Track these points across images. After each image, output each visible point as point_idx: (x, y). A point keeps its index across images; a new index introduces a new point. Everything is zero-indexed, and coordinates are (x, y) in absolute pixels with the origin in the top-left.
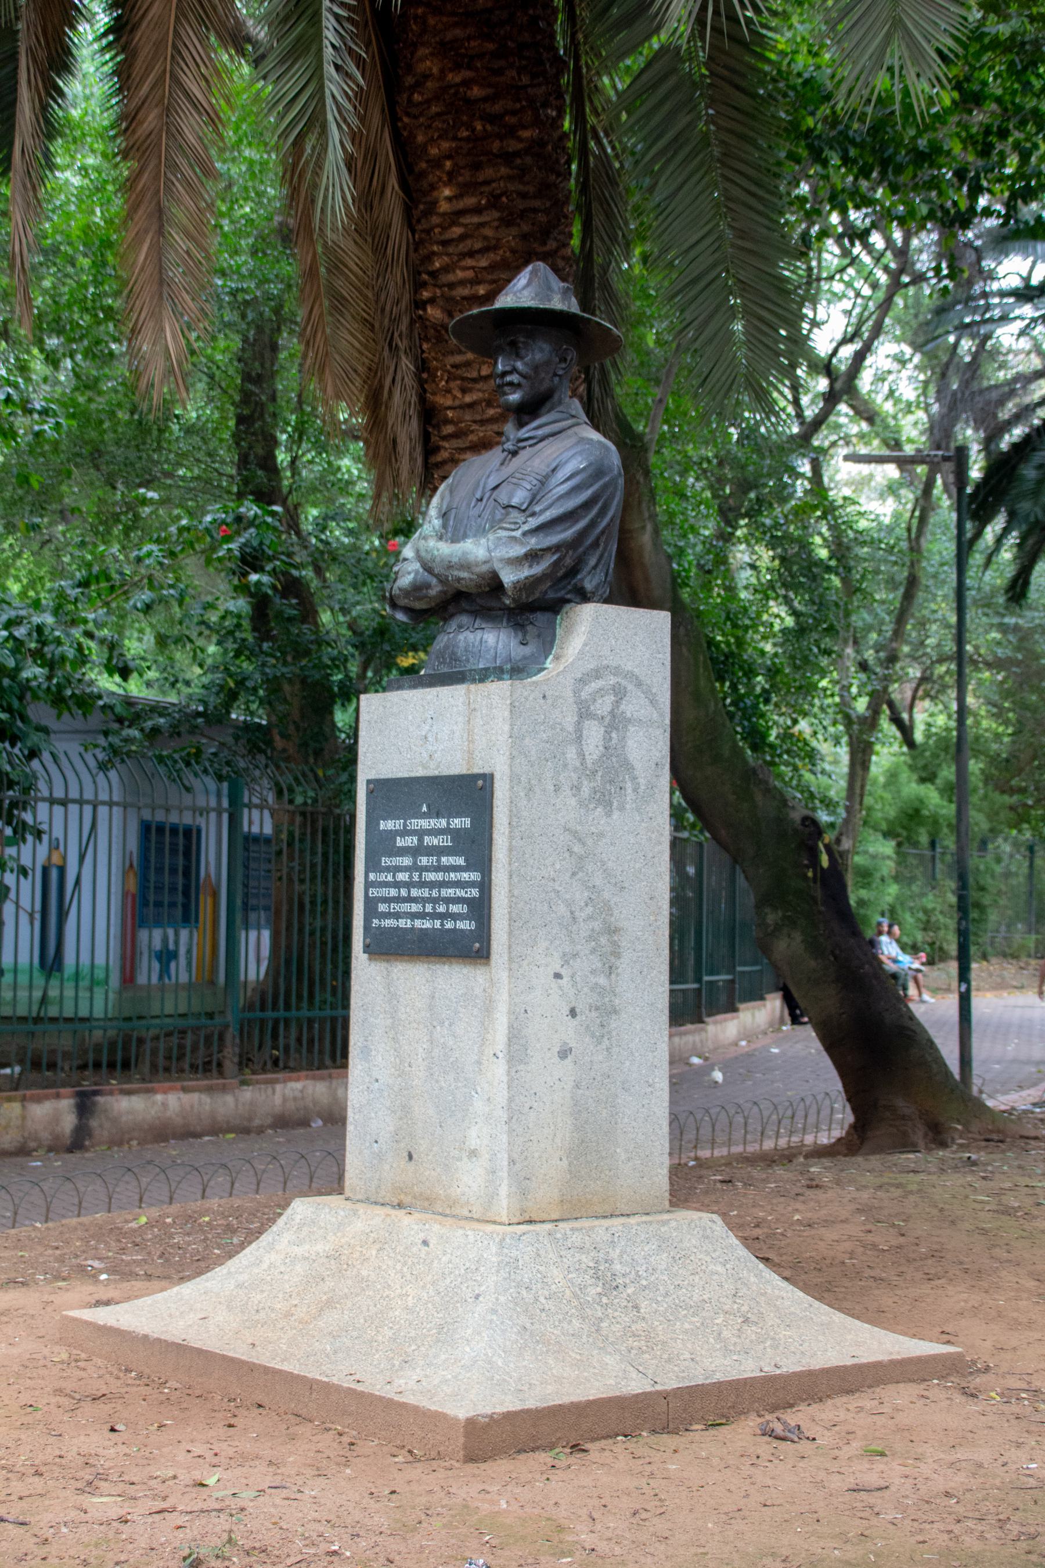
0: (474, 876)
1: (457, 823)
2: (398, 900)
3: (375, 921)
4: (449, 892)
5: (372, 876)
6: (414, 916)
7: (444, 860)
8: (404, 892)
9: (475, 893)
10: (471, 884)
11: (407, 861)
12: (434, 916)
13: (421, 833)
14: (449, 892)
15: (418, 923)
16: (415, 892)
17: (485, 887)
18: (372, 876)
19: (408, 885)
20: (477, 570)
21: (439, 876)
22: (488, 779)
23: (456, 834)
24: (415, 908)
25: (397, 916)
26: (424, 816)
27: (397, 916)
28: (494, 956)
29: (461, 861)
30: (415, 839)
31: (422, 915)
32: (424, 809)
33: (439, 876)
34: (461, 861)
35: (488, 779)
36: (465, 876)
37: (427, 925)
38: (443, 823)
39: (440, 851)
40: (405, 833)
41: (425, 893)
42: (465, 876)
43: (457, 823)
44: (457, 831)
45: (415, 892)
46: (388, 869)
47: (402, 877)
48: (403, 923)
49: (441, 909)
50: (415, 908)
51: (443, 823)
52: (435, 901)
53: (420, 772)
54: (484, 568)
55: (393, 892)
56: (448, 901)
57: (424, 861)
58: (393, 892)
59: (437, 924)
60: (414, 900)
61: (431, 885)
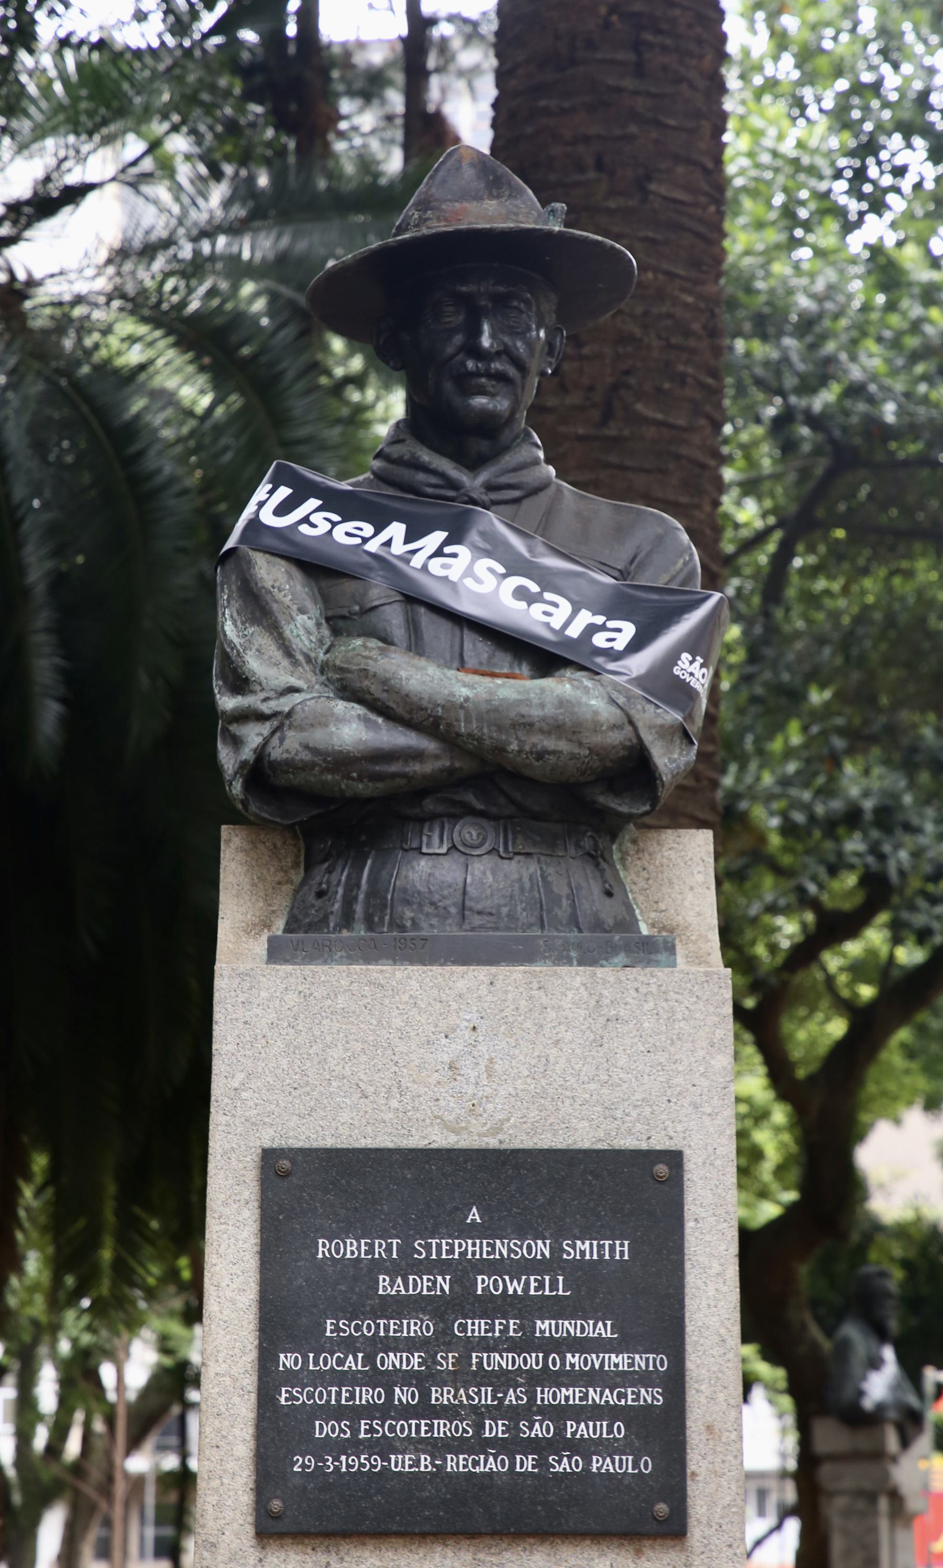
0: (656, 1362)
1: (586, 1249)
2: (386, 1411)
3: (301, 1463)
4: (570, 1395)
5: (287, 1360)
6: (438, 1448)
7: (544, 1326)
8: (402, 1395)
9: (651, 1396)
10: (644, 1379)
11: (413, 1328)
12: (511, 1446)
13: (464, 1271)
14: (570, 1395)
15: (455, 1463)
16: (441, 1396)
17: (675, 1383)
18: (287, 1360)
19: (422, 1381)
20: (597, 739)
21: (533, 1361)
22: (675, 1159)
23: (581, 1272)
24: (442, 1428)
25: (384, 1448)
26: (471, 1232)
27: (384, 1448)
28: (696, 1533)
29: (604, 1330)
30: (444, 1284)
31: (479, 1445)
32: (474, 1215)
33: (533, 1361)
34: (604, 1330)
35: (675, 1159)
36: (619, 1361)
37: (491, 1464)
38: (542, 1248)
39: (526, 1308)
40: (405, 1266)
41: (486, 1396)
42: (619, 1361)
43: (586, 1249)
44: (581, 1265)
45: (441, 1396)
46: (349, 1345)
47: (392, 1360)
48: (401, 1463)
49: (539, 1430)
50: (442, 1428)
51: (542, 1248)
52: (514, 1414)
53: (440, 1139)
54: (615, 738)
55: (365, 1396)
56: (560, 1413)
57: (477, 1327)
58: (365, 1396)
59: (528, 1464)
60: (449, 1412)
61: (502, 1380)
